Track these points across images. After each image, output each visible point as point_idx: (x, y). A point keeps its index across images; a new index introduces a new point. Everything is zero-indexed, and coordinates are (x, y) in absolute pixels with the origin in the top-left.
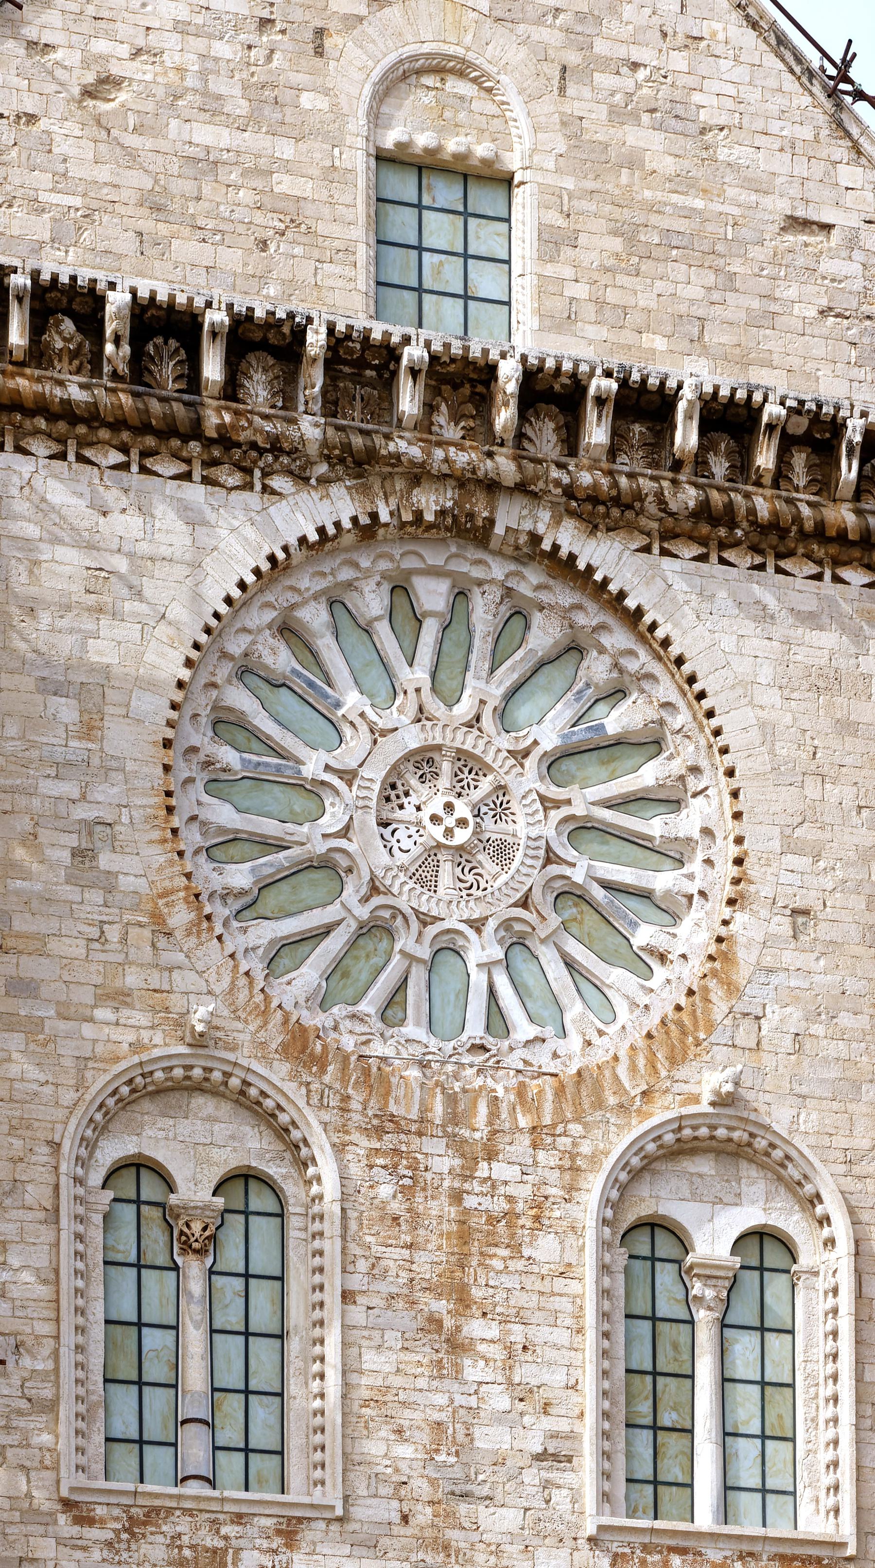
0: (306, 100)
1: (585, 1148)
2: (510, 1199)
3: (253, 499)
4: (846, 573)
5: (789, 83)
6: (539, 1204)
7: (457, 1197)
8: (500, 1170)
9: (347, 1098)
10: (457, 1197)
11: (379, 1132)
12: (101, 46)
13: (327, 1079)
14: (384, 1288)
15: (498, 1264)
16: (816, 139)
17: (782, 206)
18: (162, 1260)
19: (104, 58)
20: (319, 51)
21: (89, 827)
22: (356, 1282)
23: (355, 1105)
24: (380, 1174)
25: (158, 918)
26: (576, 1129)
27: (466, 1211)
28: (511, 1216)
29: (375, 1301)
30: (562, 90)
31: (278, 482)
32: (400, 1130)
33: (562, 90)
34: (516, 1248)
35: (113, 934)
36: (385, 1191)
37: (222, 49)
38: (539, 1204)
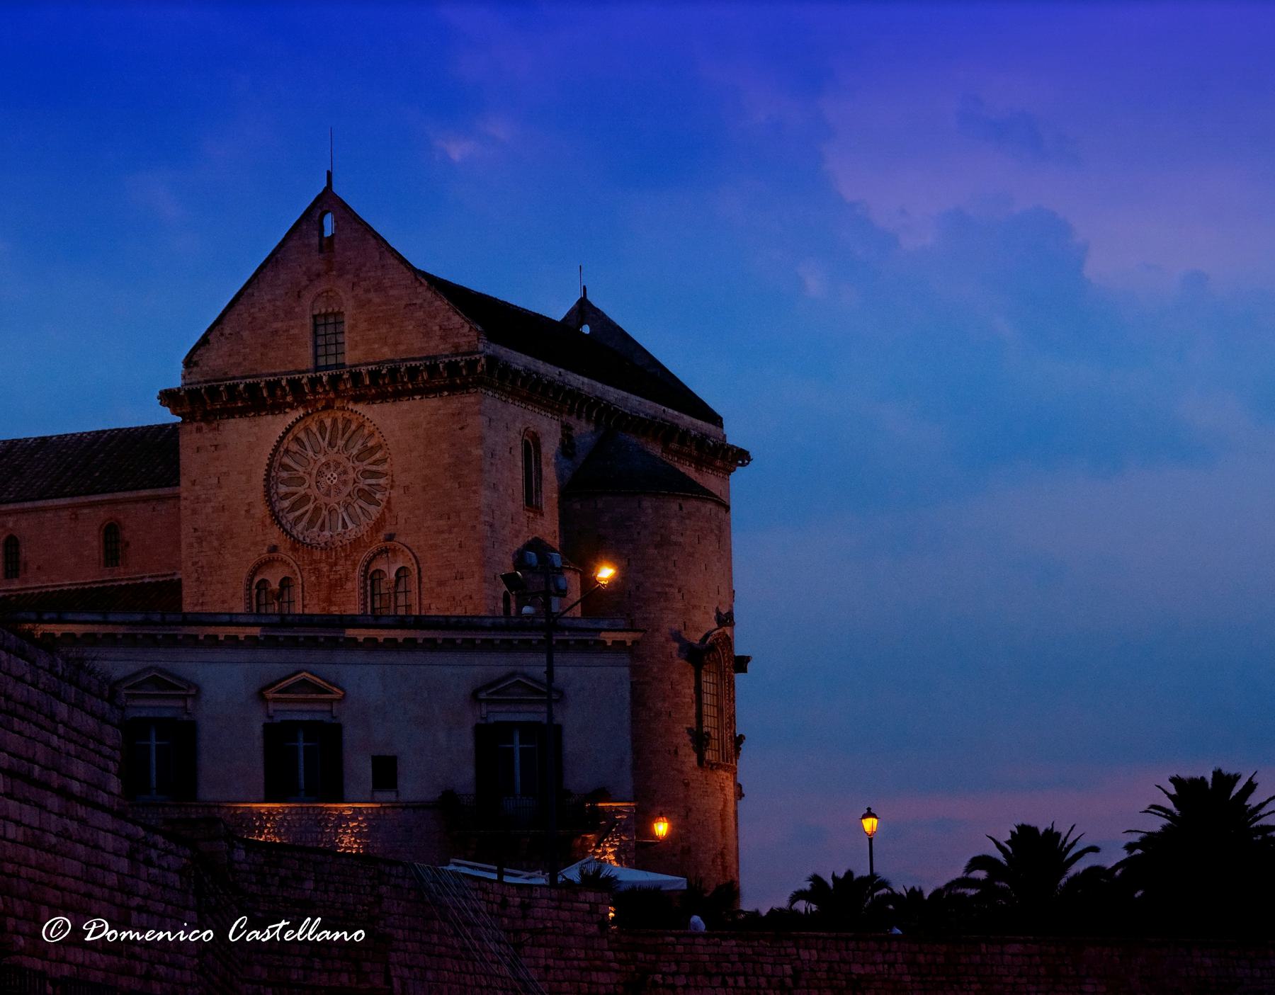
0: (296, 310)
1: (357, 558)
2: (340, 574)
3: (282, 416)
4: (415, 397)
5: (405, 270)
6: (347, 574)
7: (328, 577)
8: (339, 568)
9: (304, 557)
10: (328, 577)
11: (311, 564)
12: (252, 311)
13: (299, 553)
14: (313, 603)
15: (338, 591)
16: (412, 282)
17: (404, 303)
18: (271, 602)
19: (253, 313)
20: (299, 297)
21: (249, 504)
22: (306, 602)
23: (306, 558)
24: (312, 575)
25: (263, 522)
26: (355, 554)
27: (331, 580)
28: (341, 579)
29: (311, 606)
30: (353, 289)
31: (287, 410)
32: (316, 563)
33: (353, 289)
34: (342, 586)
35: (254, 529)
36: (313, 578)
37: (278, 303)
38: (347, 574)
